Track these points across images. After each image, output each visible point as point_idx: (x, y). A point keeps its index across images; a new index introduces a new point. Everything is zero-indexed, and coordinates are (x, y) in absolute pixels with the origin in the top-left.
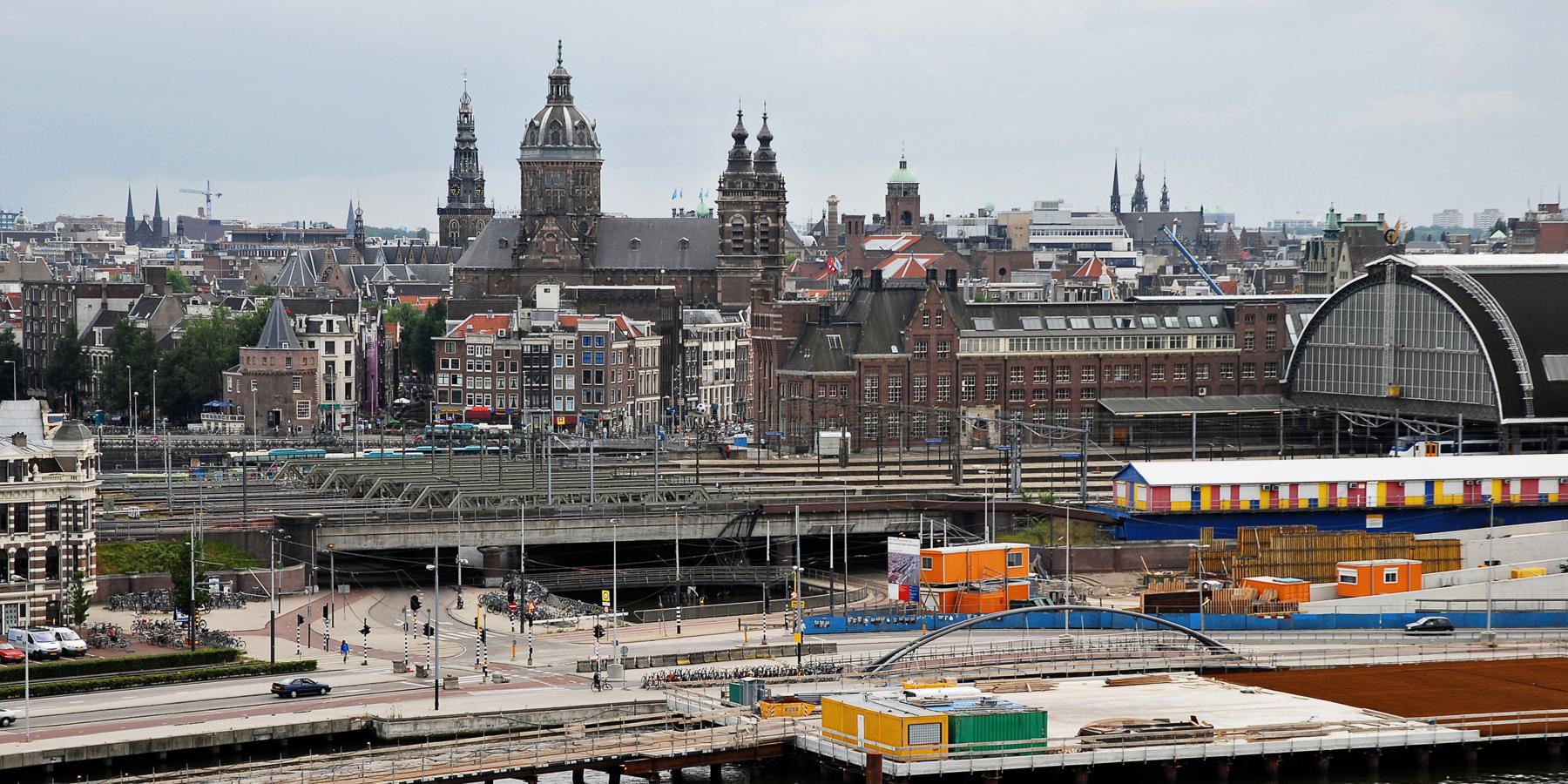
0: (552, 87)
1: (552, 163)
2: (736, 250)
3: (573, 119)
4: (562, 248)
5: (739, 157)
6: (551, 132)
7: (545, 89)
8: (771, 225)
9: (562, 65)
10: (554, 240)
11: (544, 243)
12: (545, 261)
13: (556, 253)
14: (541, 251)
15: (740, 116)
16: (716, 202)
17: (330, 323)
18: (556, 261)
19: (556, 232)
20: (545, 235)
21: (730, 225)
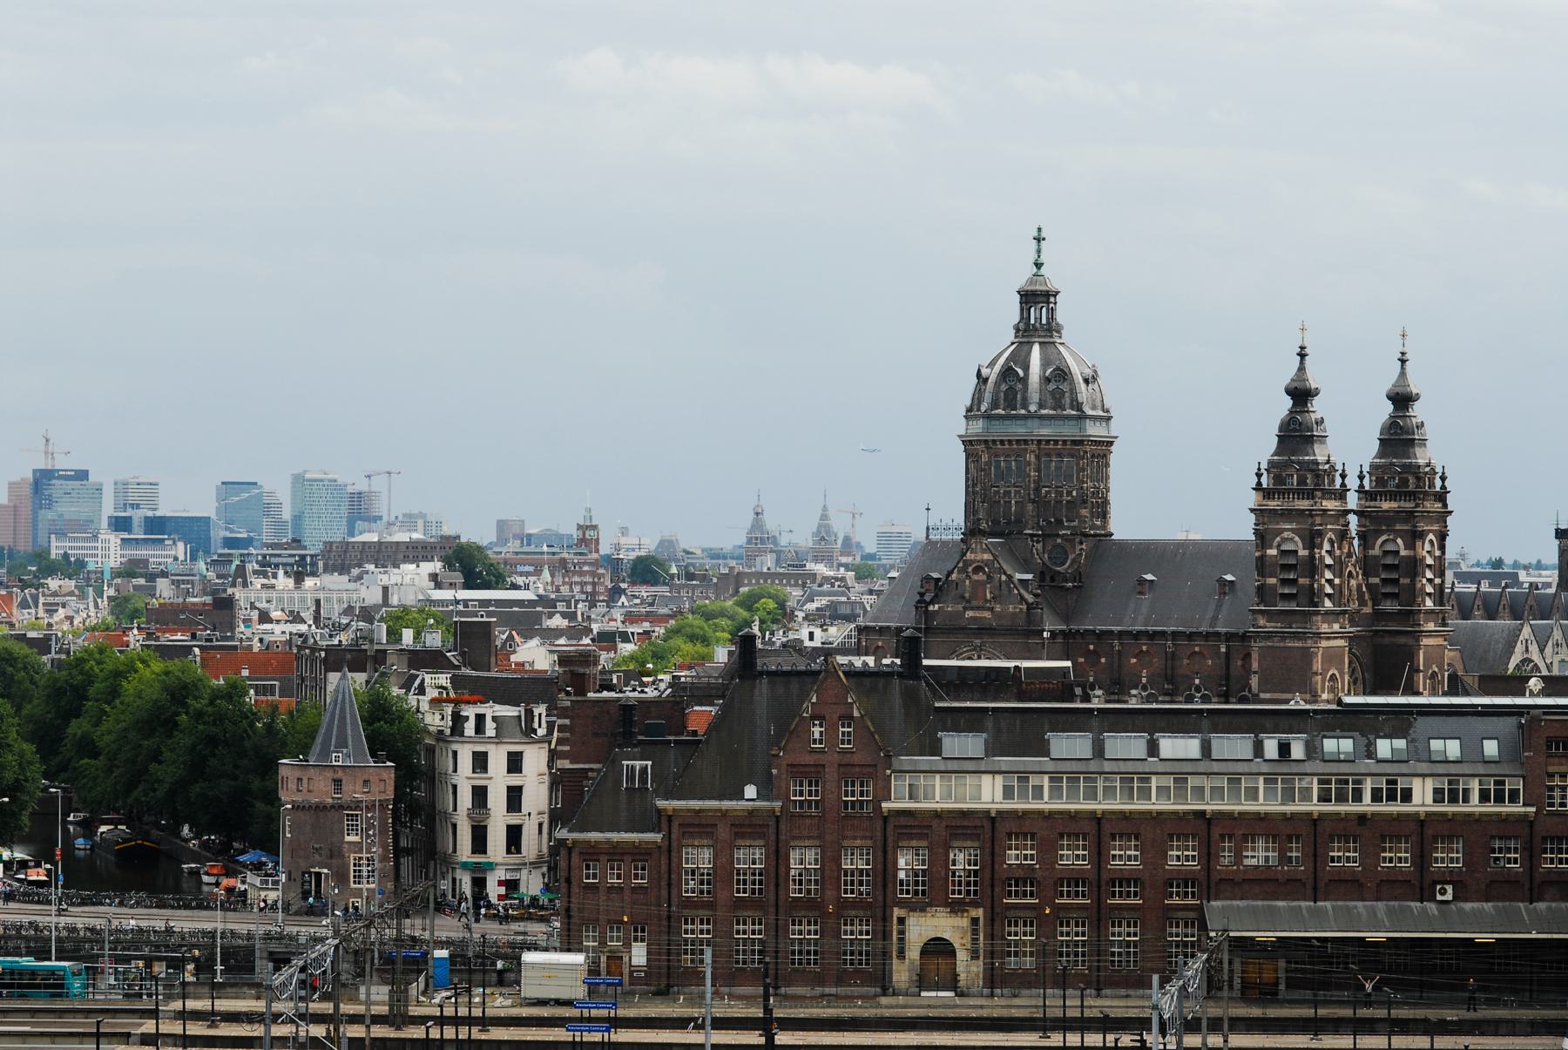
0: (1022, 310)
1: (1002, 442)
2: (1285, 597)
3: (1045, 363)
4: (997, 592)
5: (1295, 430)
6: (1004, 387)
7: (1011, 312)
8: (1403, 553)
9: (1043, 271)
10: (985, 577)
11: (967, 582)
12: (970, 614)
13: (987, 601)
14: (963, 597)
15: (1302, 356)
16: (1252, 510)
17: (480, 719)
18: (987, 614)
19: (987, 563)
20: (970, 569)
21: (1273, 552)
